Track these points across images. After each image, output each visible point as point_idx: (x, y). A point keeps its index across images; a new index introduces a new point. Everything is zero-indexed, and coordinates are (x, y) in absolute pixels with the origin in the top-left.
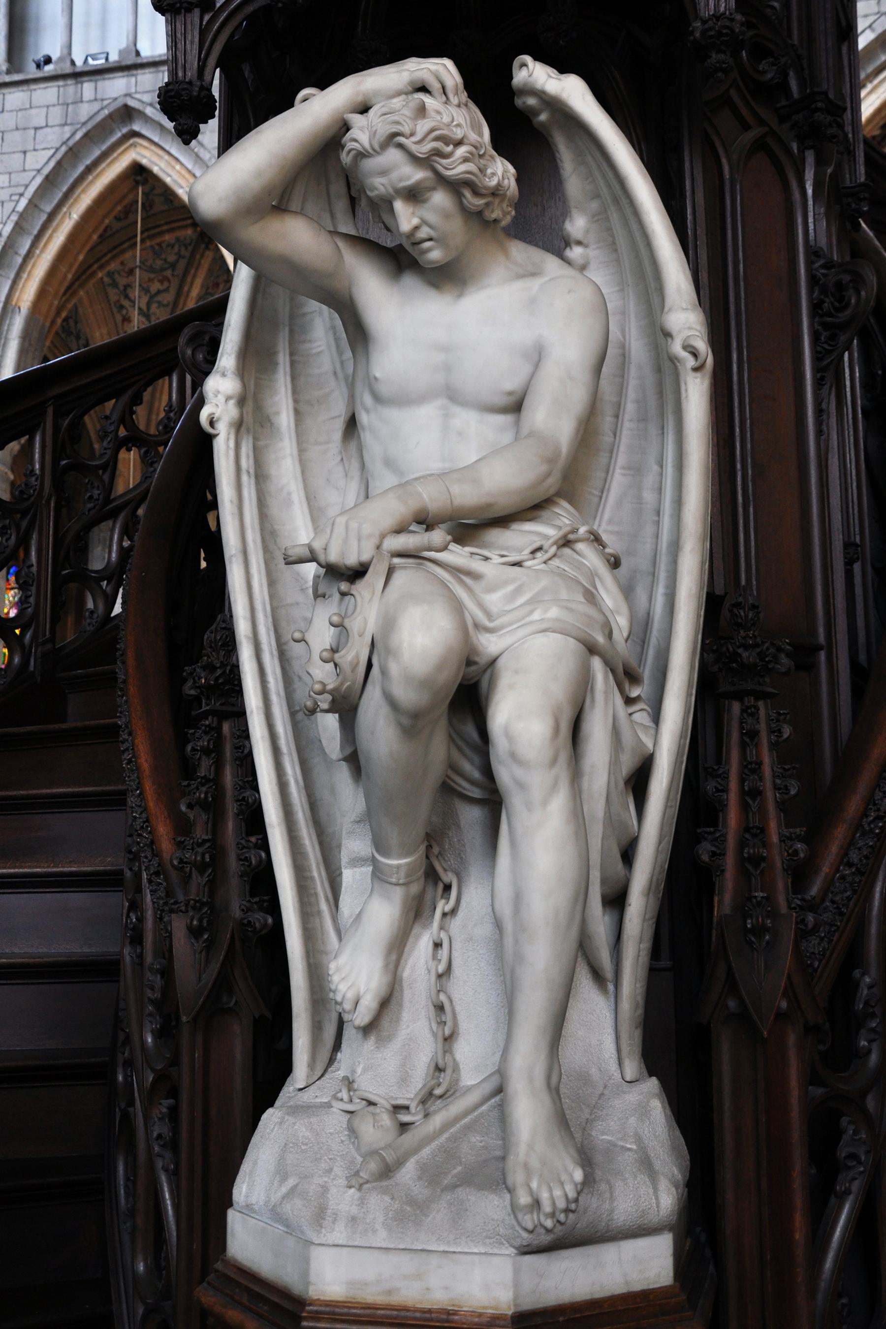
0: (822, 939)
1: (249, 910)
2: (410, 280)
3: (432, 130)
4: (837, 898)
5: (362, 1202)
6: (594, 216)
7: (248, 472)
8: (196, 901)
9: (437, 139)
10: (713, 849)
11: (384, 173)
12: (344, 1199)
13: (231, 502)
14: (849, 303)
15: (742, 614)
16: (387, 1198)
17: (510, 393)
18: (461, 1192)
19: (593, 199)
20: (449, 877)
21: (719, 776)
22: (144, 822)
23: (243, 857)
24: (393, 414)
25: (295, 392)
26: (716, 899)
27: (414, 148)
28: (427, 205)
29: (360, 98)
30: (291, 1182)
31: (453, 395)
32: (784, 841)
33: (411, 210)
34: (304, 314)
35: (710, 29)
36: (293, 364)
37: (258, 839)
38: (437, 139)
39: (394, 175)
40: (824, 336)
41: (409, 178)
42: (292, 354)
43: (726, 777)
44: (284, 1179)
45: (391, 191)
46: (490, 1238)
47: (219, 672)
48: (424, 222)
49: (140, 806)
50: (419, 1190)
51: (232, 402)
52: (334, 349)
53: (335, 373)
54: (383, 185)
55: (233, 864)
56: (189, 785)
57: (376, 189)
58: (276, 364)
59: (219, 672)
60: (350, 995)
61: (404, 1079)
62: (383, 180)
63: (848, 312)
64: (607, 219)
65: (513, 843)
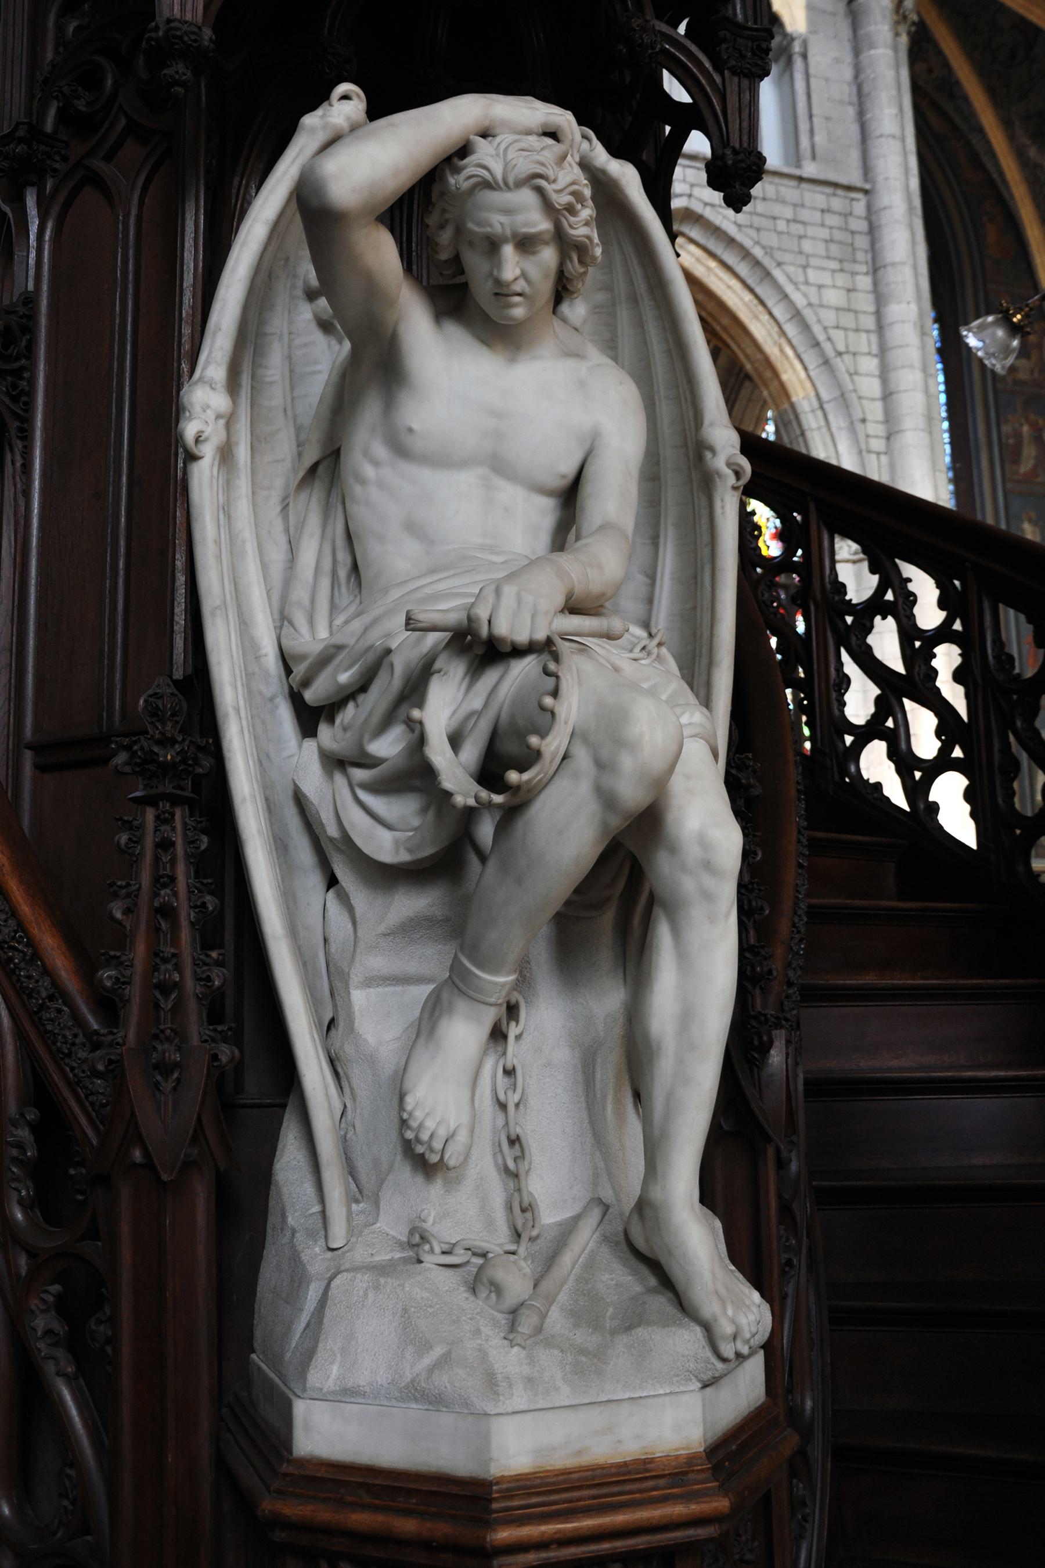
2: (454, 330)
3: (573, 183)
5: (532, 1360)
6: (596, 307)
9: (573, 194)
11: (508, 211)
12: (509, 1361)
16: (556, 1352)
17: (564, 477)
18: (641, 1332)
19: (600, 289)
22: (16, 932)
23: (204, 976)
24: (425, 474)
27: (554, 197)
28: (532, 258)
29: (487, 123)
30: (438, 1351)
31: (499, 466)
33: (517, 258)
34: (265, 334)
35: (742, 161)
38: (573, 194)
39: (520, 218)
41: (534, 225)
44: (426, 1346)
45: (508, 232)
46: (677, 1376)
48: (524, 275)
50: (584, 1337)
51: (222, 422)
52: (287, 382)
53: (285, 410)
54: (501, 224)
56: (128, 885)
57: (491, 226)
58: (240, 386)
61: (490, 1224)
62: (503, 219)
64: (613, 315)
65: (683, 957)
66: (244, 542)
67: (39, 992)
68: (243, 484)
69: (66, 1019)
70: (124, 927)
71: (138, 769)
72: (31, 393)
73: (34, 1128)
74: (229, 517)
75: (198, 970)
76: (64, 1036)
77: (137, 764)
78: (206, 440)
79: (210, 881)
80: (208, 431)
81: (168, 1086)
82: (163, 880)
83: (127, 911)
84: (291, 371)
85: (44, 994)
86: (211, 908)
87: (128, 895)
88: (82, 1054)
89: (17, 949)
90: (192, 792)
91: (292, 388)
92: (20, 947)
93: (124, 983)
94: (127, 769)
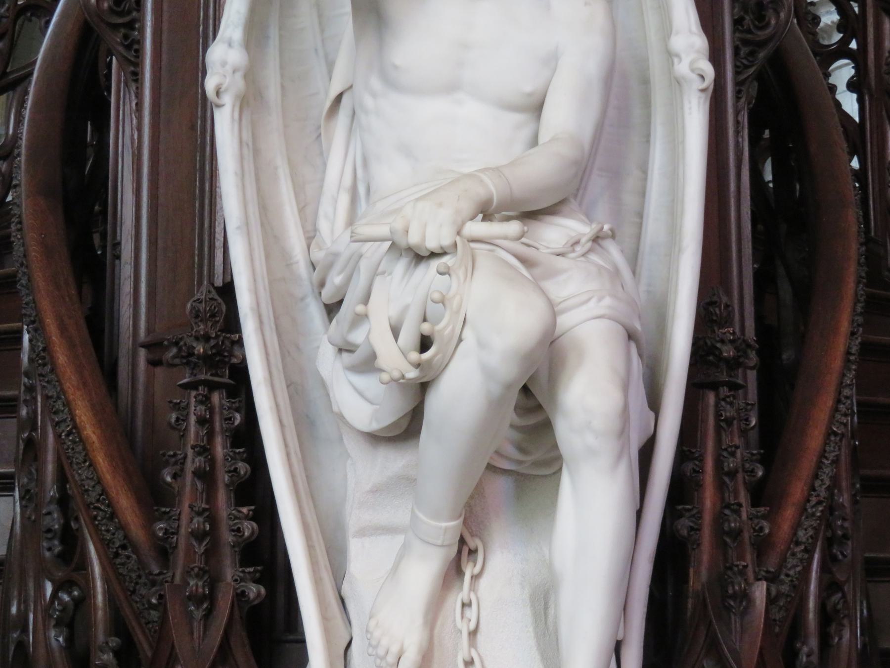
0: (781, 608)
1: (242, 580)
4: (792, 573)
7: (248, 145)
8: (200, 569)
10: (692, 524)
13: (236, 173)
14: (768, 24)
15: (718, 312)
17: (530, 95)
20: (472, 543)
21: (696, 459)
22: (101, 495)
23: (235, 528)
25: (282, 67)
26: (691, 571)
32: (751, 519)
36: (281, 37)
37: (249, 511)
40: (744, 51)
42: (280, 29)
43: (701, 459)
47: (213, 342)
49: (92, 479)
51: (239, 76)
55: (228, 537)
58: (267, 37)
59: (213, 342)
60: (394, 649)
63: (768, 31)
66: (276, 168)
67: (113, 543)
68: (274, 121)
69: (133, 563)
70: (173, 488)
71: (185, 361)
72: (140, 42)
73: (117, 653)
74: (256, 153)
75: (231, 523)
76: (130, 577)
77: (183, 357)
78: (226, 90)
79: (242, 450)
80: (227, 82)
81: (198, 614)
82: (205, 450)
83: (175, 476)
84: (320, 16)
85: (117, 544)
86: (242, 473)
87: (176, 463)
88: (143, 591)
89: (101, 510)
90: (230, 378)
91: (322, 31)
92: (103, 507)
93: (173, 533)
94: (177, 361)
